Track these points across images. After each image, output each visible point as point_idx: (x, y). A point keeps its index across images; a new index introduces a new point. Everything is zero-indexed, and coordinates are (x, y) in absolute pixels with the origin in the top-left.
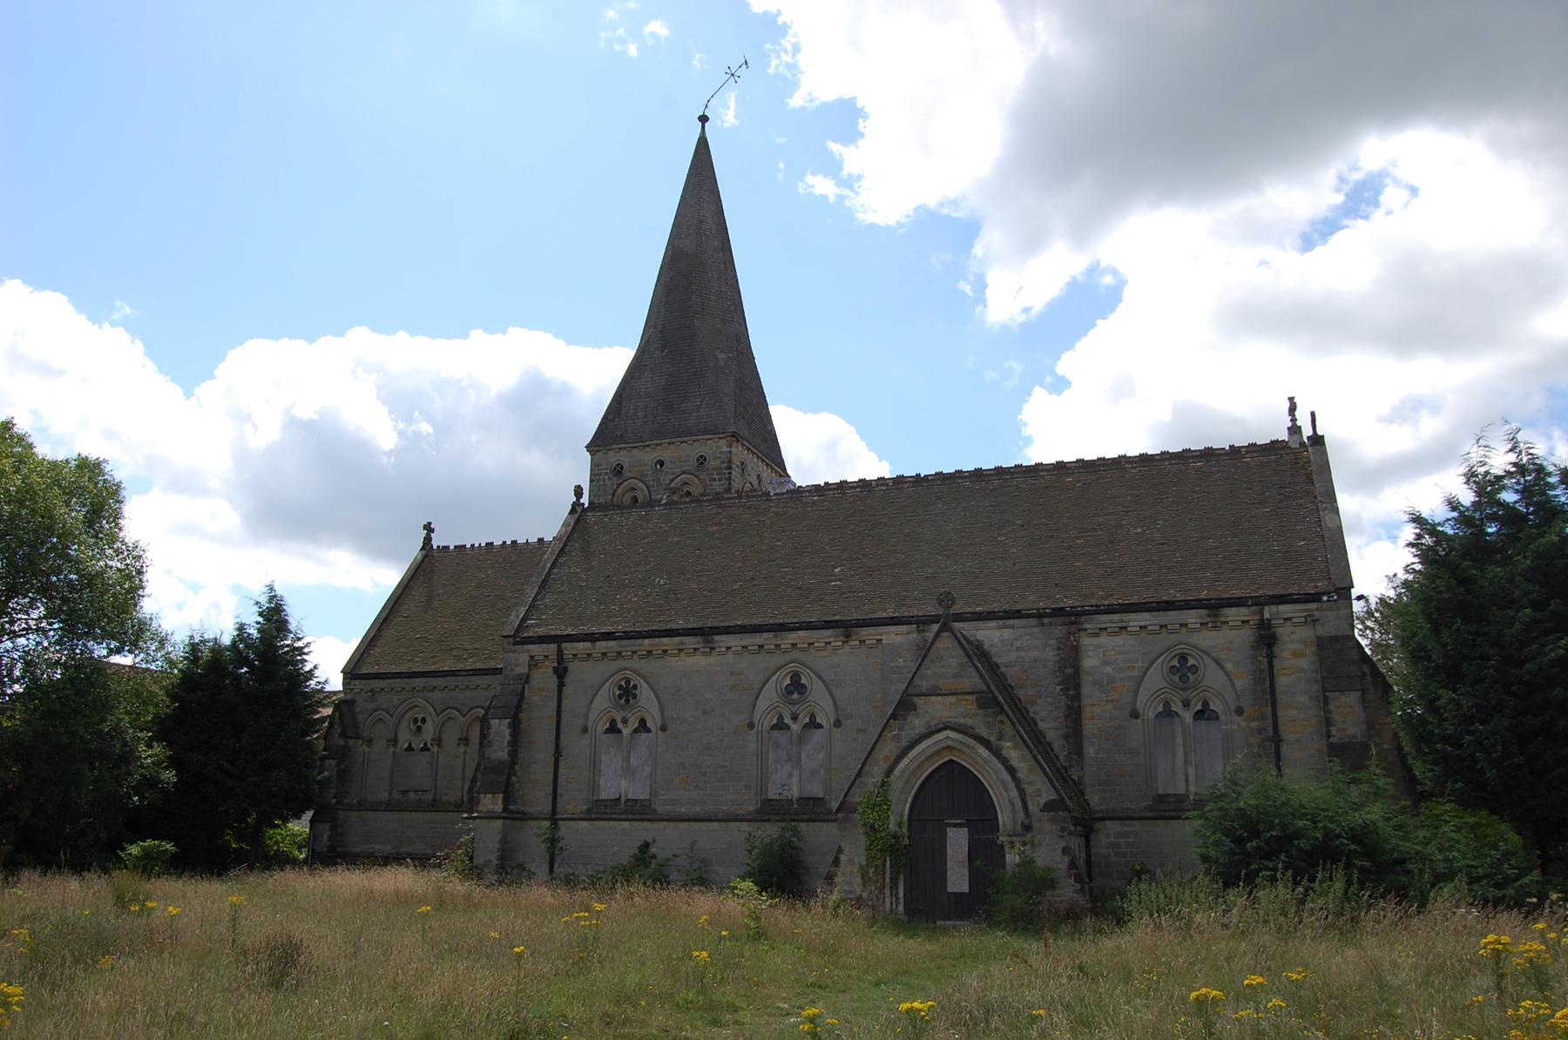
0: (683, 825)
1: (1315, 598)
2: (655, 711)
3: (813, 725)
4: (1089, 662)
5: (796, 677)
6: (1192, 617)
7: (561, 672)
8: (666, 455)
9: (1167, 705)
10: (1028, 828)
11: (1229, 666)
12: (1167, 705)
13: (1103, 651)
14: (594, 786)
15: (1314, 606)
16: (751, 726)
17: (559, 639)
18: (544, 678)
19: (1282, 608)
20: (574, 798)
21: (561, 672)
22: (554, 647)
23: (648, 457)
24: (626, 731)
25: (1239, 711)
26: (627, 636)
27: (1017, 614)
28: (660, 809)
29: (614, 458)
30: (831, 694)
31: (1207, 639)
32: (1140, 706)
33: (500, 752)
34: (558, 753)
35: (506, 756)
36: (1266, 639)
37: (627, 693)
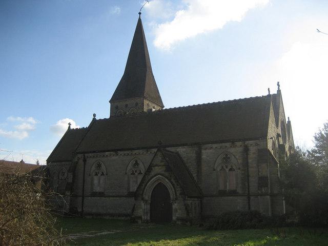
4: (204, 157)
5: (136, 161)
6: (228, 144)
7: (85, 161)
10: (176, 199)
11: (237, 157)
13: (207, 154)
16: (126, 173)
17: (84, 153)
18: (81, 162)
19: (250, 142)
21: (85, 161)
25: (239, 169)
27: (186, 145)
29: (116, 104)
31: (232, 150)
32: (215, 167)
33: (70, 181)
36: (246, 150)
37: (99, 166)
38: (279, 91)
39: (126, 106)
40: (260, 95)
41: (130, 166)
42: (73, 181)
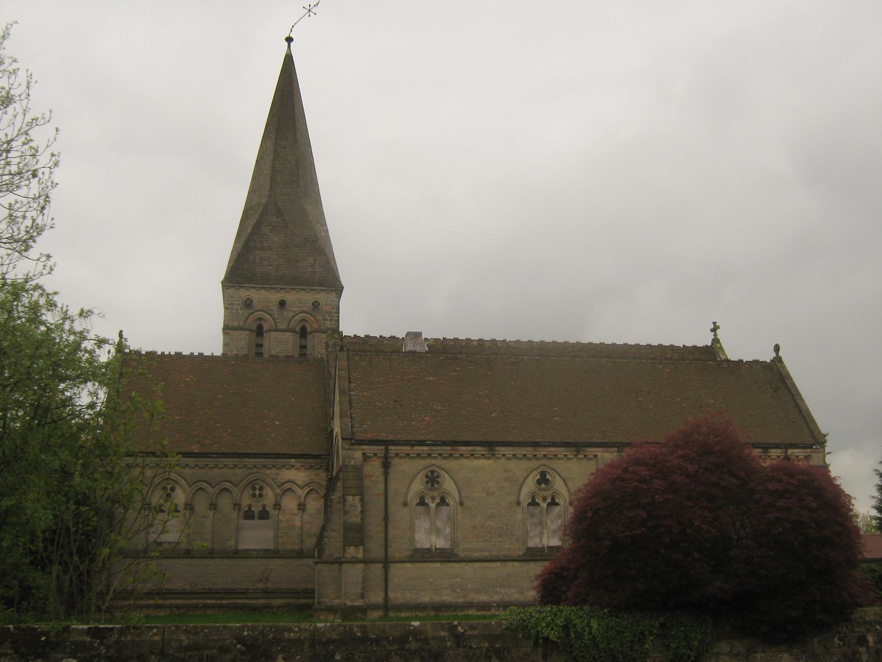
0: (477, 565)
1: (810, 446)
2: (455, 493)
3: (553, 503)
5: (543, 474)
7: (386, 466)
8: (289, 297)
9: (533, 499)
12: (533, 499)
14: (412, 540)
15: (809, 450)
16: (518, 503)
18: (374, 468)
19: (796, 450)
20: (399, 548)
21: (386, 466)
22: (383, 448)
23: (274, 297)
24: (433, 505)
26: (435, 443)
28: (461, 554)
29: (244, 293)
30: (566, 485)
34: (386, 519)
35: (359, 520)
37: (432, 480)
38: (716, 340)
39: (282, 304)
40: (700, 344)
41: (530, 486)
42: (362, 519)
